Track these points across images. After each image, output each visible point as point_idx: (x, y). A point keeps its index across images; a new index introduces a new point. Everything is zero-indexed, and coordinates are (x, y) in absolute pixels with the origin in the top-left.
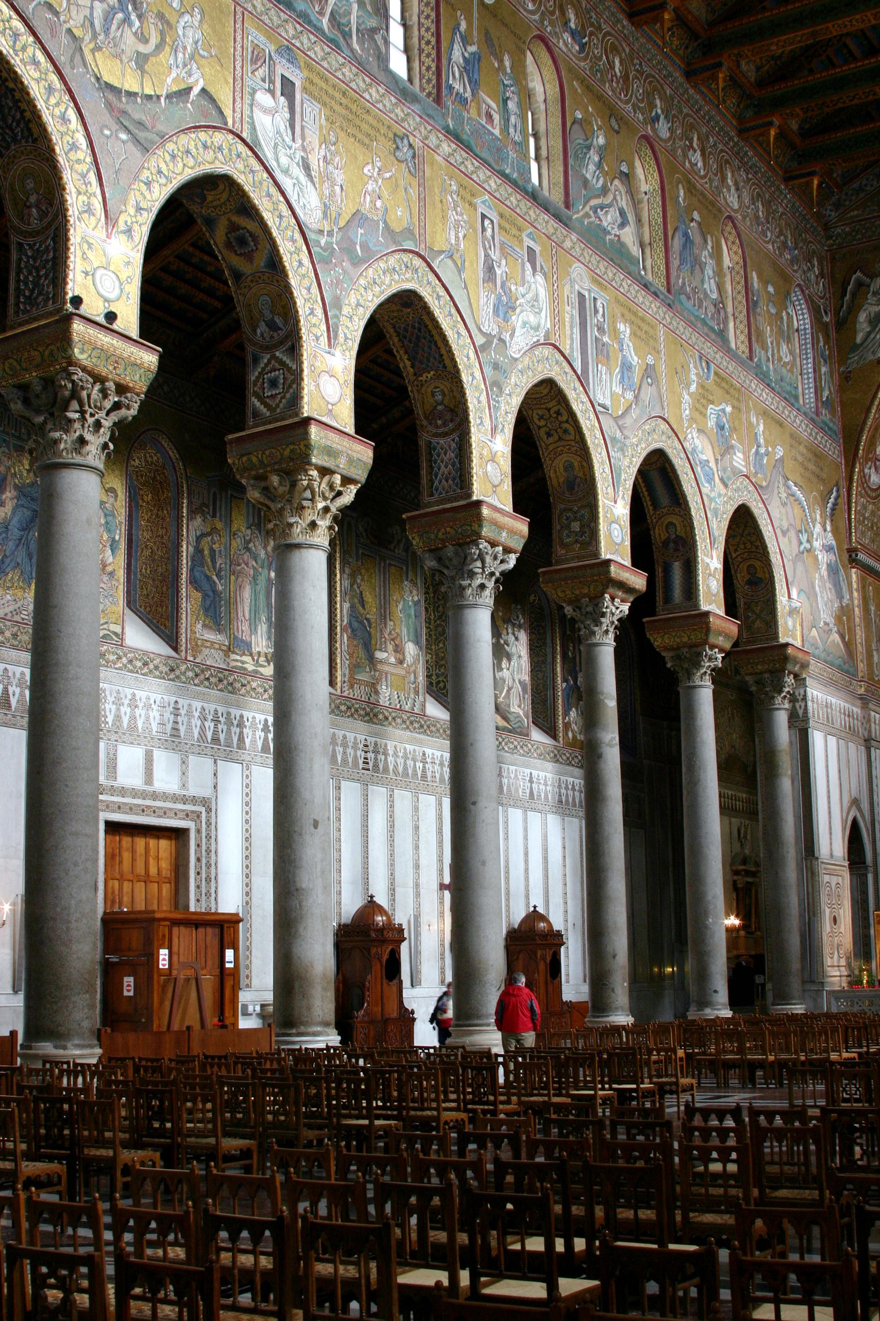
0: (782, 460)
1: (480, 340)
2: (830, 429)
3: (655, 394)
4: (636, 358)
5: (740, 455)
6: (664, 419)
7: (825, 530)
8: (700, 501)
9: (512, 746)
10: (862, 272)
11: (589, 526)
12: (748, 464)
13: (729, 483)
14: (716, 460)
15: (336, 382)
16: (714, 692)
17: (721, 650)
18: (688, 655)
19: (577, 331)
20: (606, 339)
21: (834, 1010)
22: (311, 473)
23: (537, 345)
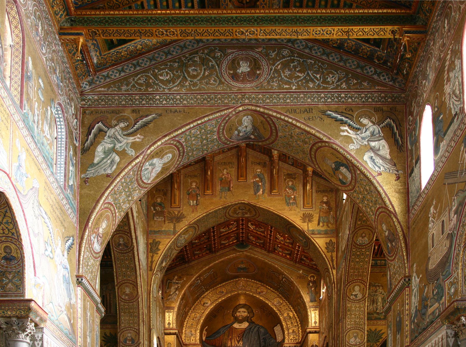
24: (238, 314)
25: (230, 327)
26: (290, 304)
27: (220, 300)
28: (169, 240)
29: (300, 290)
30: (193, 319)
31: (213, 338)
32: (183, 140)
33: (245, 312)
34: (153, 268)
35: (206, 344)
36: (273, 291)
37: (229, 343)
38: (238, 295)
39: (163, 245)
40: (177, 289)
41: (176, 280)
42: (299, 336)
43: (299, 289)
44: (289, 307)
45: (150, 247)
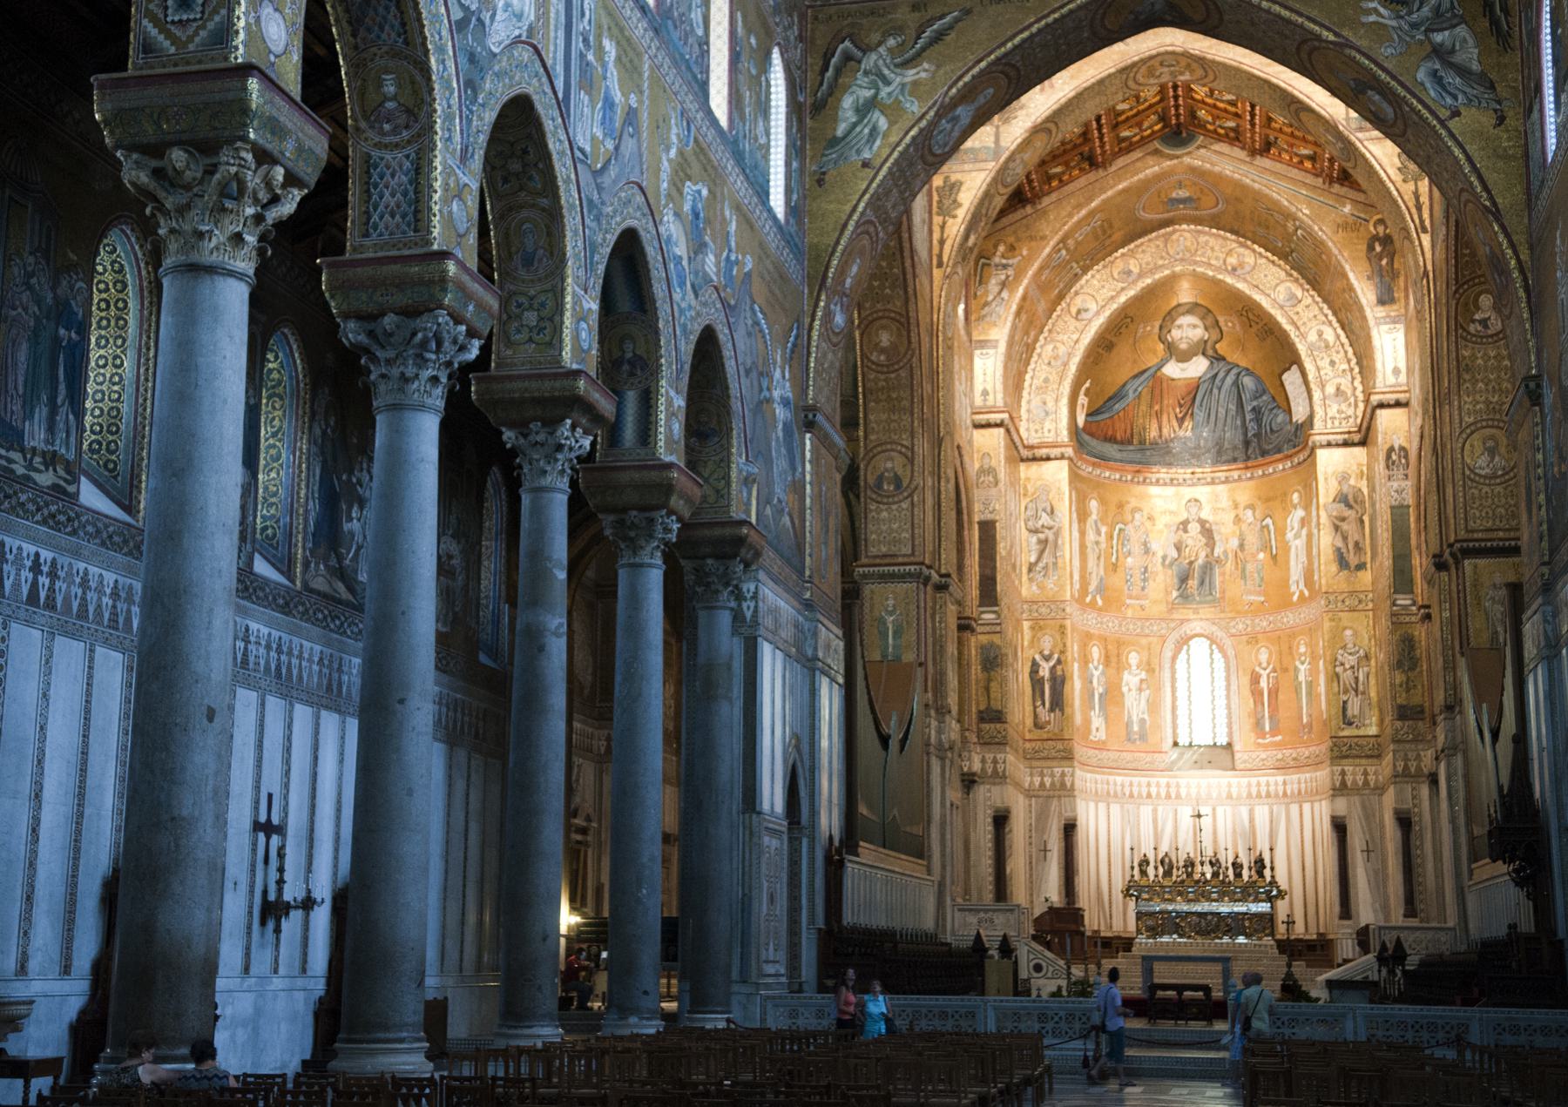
0: (748, 275)
1: (457, 14)
2: (796, 245)
3: (635, 149)
4: (619, 94)
5: (711, 257)
6: (641, 188)
7: (784, 377)
8: (669, 311)
9: (356, 630)
10: (853, 42)
11: (551, 320)
12: (718, 274)
13: (700, 293)
14: (690, 258)
15: (281, 22)
16: (666, 575)
17: (679, 520)
18: (636, 521)
19: (561, 34)
20: (590, 57)
21: (772, 1024)
22: (244, 154)
23: (517, 41)
24: (1176, 334)
25: (1153, 376)
26: (1325, 301)
27: (1123, 299)
28: (983, 175)
29: (1347, 267)
30: (1049, 363)
31: (1106, 415)
32: (1018, 58)
33: (1195, 326)
34: (945, 259)
35: (1086, 437)
36: (1273, 262)
37: (1155, 426)
38: (1173, 279)
39: (968, 189)
40: (1003, 285)
41: (1003, 256)
42: (1356, 406)
43: (1343, 262)
44: (1321, 309)
45: (936, 198)
